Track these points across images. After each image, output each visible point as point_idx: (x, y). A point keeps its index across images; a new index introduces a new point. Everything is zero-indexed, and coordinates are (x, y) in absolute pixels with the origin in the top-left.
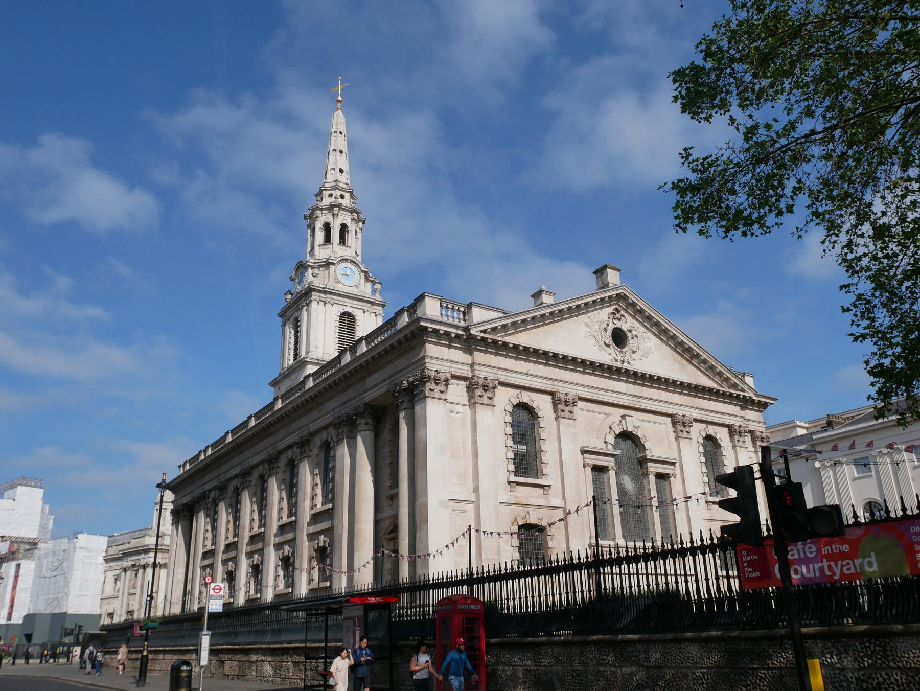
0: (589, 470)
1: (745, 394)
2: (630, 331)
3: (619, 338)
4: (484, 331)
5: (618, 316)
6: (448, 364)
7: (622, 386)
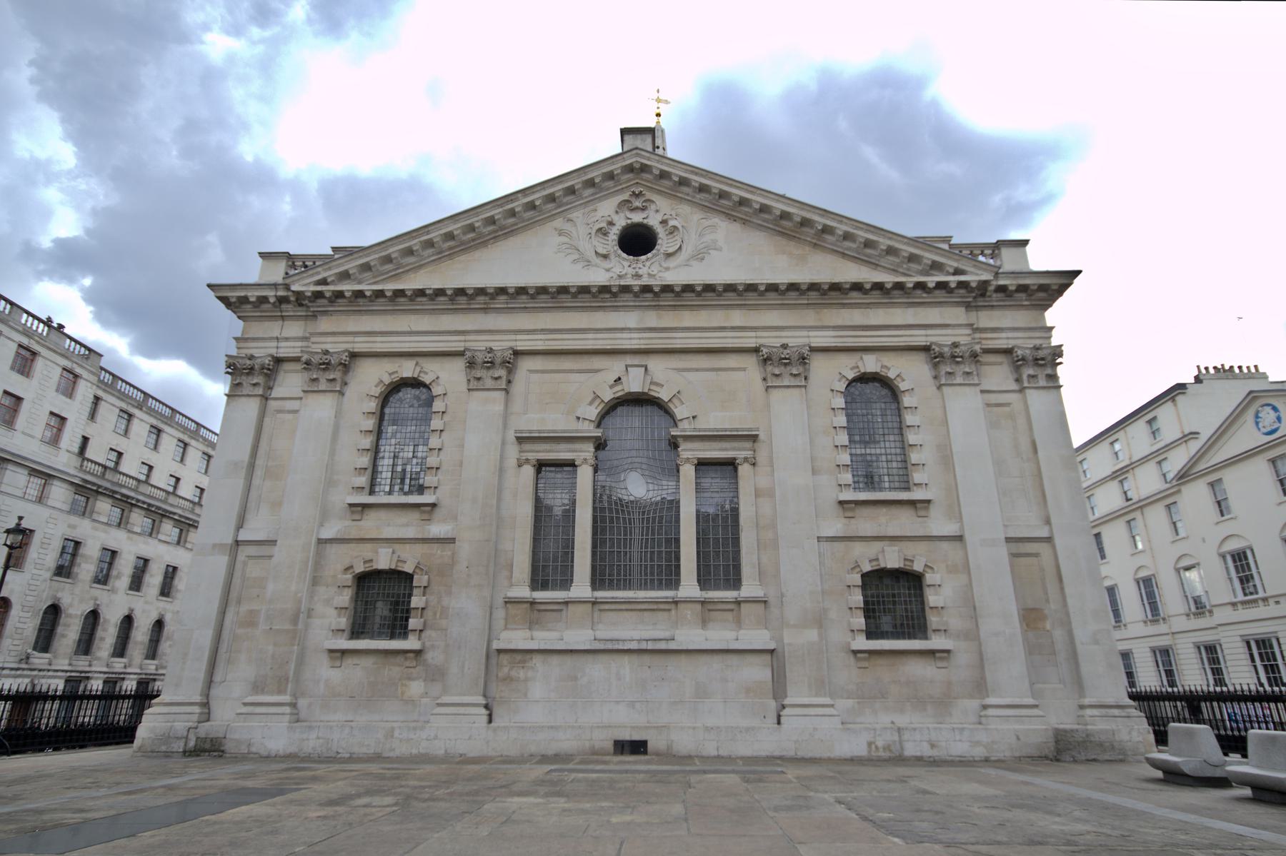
0: (529, 471)
1: (962, 278)
2: (664, 222)
3: (637, 241)
4: (324, 282)
5: (637, 203)
6: (274, 344)
7: (630, 319)
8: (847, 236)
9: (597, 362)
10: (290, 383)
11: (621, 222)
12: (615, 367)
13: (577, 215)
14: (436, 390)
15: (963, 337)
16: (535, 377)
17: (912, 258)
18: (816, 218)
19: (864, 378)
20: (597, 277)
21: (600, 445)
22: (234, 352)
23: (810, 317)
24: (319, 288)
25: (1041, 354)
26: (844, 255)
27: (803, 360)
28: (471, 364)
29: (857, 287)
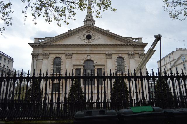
2: (92, 35)
3: (89, 37)
4: (45, 43)
7: (88, 49)
8: (118, 37)
9: (84, 55)
10: (40, 57)
11: (86, 34)
12: (86, 56)
13: (80, 33)
14: (62, 59)
15: (132, 52)
16: (75, 57)
17: (126, 41)
18: (113, 35)
19: (119, 57)
20: (83, 43)
21: (84, 66)
22: (32, 53)
23: (112, 49)
24: (44, 44)
25: (143, 54)
26: (117, 40)
27: (111, 55)
28: (66, 55)
29: (119, 45)
